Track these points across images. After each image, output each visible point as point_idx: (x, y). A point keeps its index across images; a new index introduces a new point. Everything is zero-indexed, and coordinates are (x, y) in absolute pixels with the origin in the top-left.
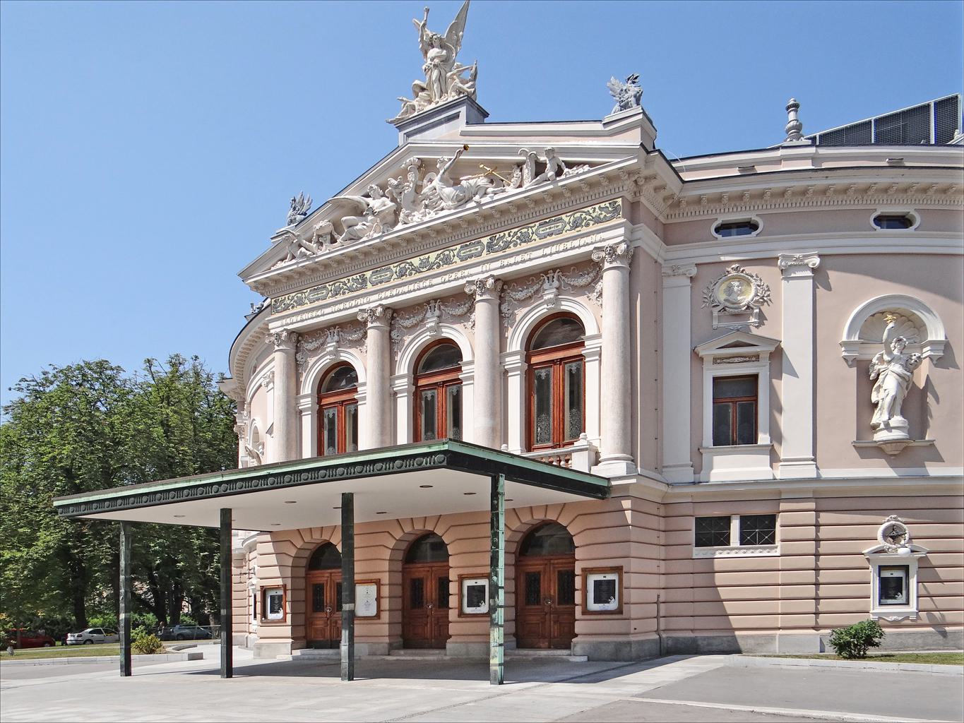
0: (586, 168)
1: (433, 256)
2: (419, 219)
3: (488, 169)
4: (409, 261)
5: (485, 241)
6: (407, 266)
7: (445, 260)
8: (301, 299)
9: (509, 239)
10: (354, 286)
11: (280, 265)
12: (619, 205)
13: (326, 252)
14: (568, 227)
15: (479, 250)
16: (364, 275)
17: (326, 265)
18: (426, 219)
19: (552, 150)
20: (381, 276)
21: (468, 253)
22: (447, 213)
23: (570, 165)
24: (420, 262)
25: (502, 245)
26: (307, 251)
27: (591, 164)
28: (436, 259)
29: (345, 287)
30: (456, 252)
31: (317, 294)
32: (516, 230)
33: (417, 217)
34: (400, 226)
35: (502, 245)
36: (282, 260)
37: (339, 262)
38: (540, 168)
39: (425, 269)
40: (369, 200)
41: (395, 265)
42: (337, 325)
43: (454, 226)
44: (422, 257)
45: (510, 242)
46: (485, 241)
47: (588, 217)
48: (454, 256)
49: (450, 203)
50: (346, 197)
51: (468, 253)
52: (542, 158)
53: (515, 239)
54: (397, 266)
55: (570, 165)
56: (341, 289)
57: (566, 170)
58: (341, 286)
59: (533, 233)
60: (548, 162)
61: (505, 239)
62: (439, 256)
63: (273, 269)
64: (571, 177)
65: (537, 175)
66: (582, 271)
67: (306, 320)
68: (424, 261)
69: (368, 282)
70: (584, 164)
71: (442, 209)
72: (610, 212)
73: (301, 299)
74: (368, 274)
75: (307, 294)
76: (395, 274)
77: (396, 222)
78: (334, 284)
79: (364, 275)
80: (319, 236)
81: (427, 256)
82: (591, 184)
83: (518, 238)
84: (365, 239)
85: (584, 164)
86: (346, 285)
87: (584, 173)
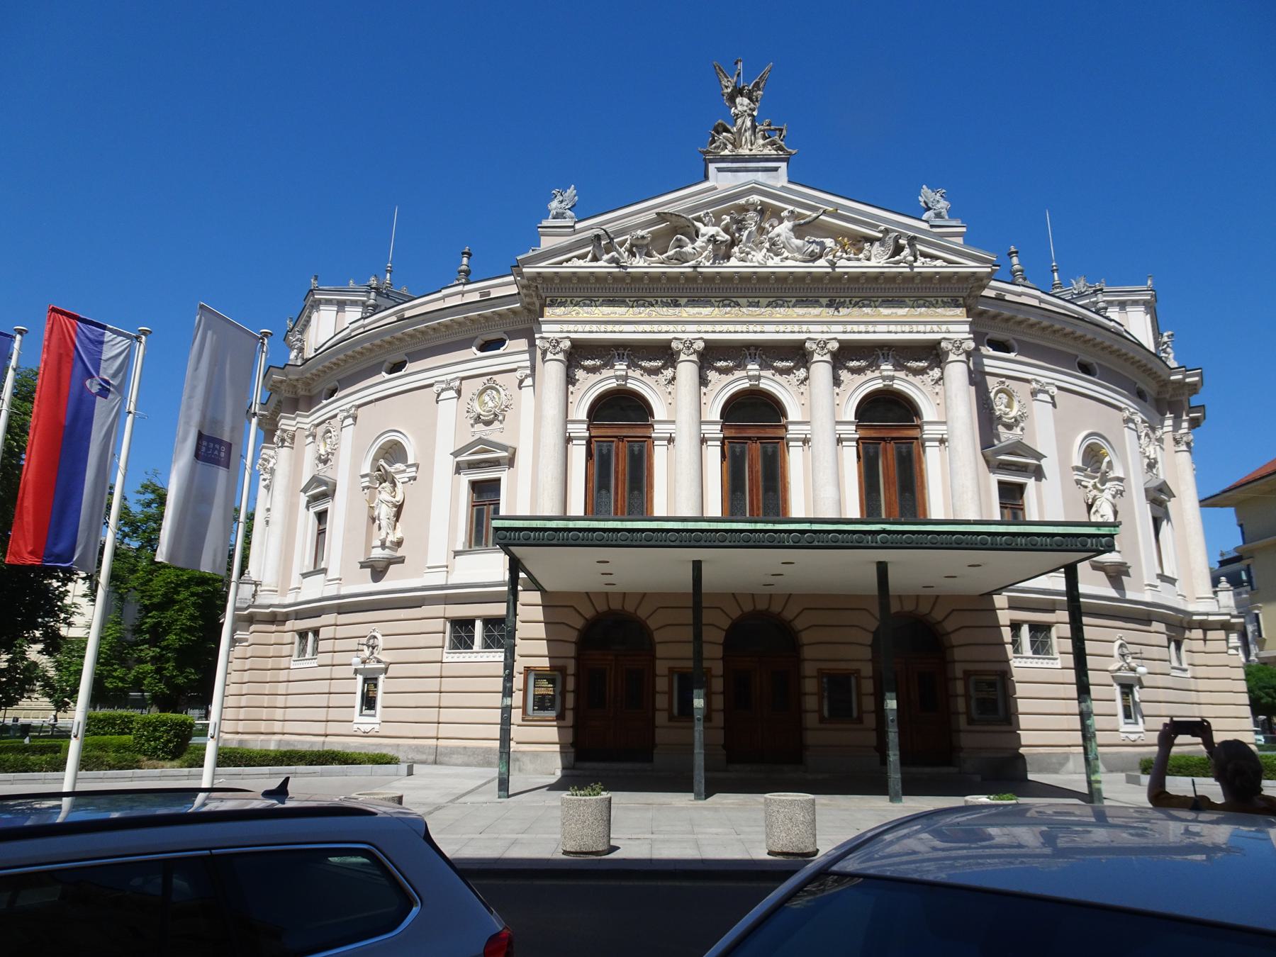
0: (939, 263)
2: (757, 260)
11: (576, 262)
13: (639, 264)
19: (914, 238)
23: (924, 255)
27: (945, 260)
33: (758, 256)
34: (733, 262)
36: (579, 257)
37: (654, 279)
49: (800, 257)
55: (924, 255)
64: (923, 266)
66: (932, 354)
70: (937, 258)
71: (787, 258)
77: (728, 257)
80: (632, 245)
85: (937, 258)
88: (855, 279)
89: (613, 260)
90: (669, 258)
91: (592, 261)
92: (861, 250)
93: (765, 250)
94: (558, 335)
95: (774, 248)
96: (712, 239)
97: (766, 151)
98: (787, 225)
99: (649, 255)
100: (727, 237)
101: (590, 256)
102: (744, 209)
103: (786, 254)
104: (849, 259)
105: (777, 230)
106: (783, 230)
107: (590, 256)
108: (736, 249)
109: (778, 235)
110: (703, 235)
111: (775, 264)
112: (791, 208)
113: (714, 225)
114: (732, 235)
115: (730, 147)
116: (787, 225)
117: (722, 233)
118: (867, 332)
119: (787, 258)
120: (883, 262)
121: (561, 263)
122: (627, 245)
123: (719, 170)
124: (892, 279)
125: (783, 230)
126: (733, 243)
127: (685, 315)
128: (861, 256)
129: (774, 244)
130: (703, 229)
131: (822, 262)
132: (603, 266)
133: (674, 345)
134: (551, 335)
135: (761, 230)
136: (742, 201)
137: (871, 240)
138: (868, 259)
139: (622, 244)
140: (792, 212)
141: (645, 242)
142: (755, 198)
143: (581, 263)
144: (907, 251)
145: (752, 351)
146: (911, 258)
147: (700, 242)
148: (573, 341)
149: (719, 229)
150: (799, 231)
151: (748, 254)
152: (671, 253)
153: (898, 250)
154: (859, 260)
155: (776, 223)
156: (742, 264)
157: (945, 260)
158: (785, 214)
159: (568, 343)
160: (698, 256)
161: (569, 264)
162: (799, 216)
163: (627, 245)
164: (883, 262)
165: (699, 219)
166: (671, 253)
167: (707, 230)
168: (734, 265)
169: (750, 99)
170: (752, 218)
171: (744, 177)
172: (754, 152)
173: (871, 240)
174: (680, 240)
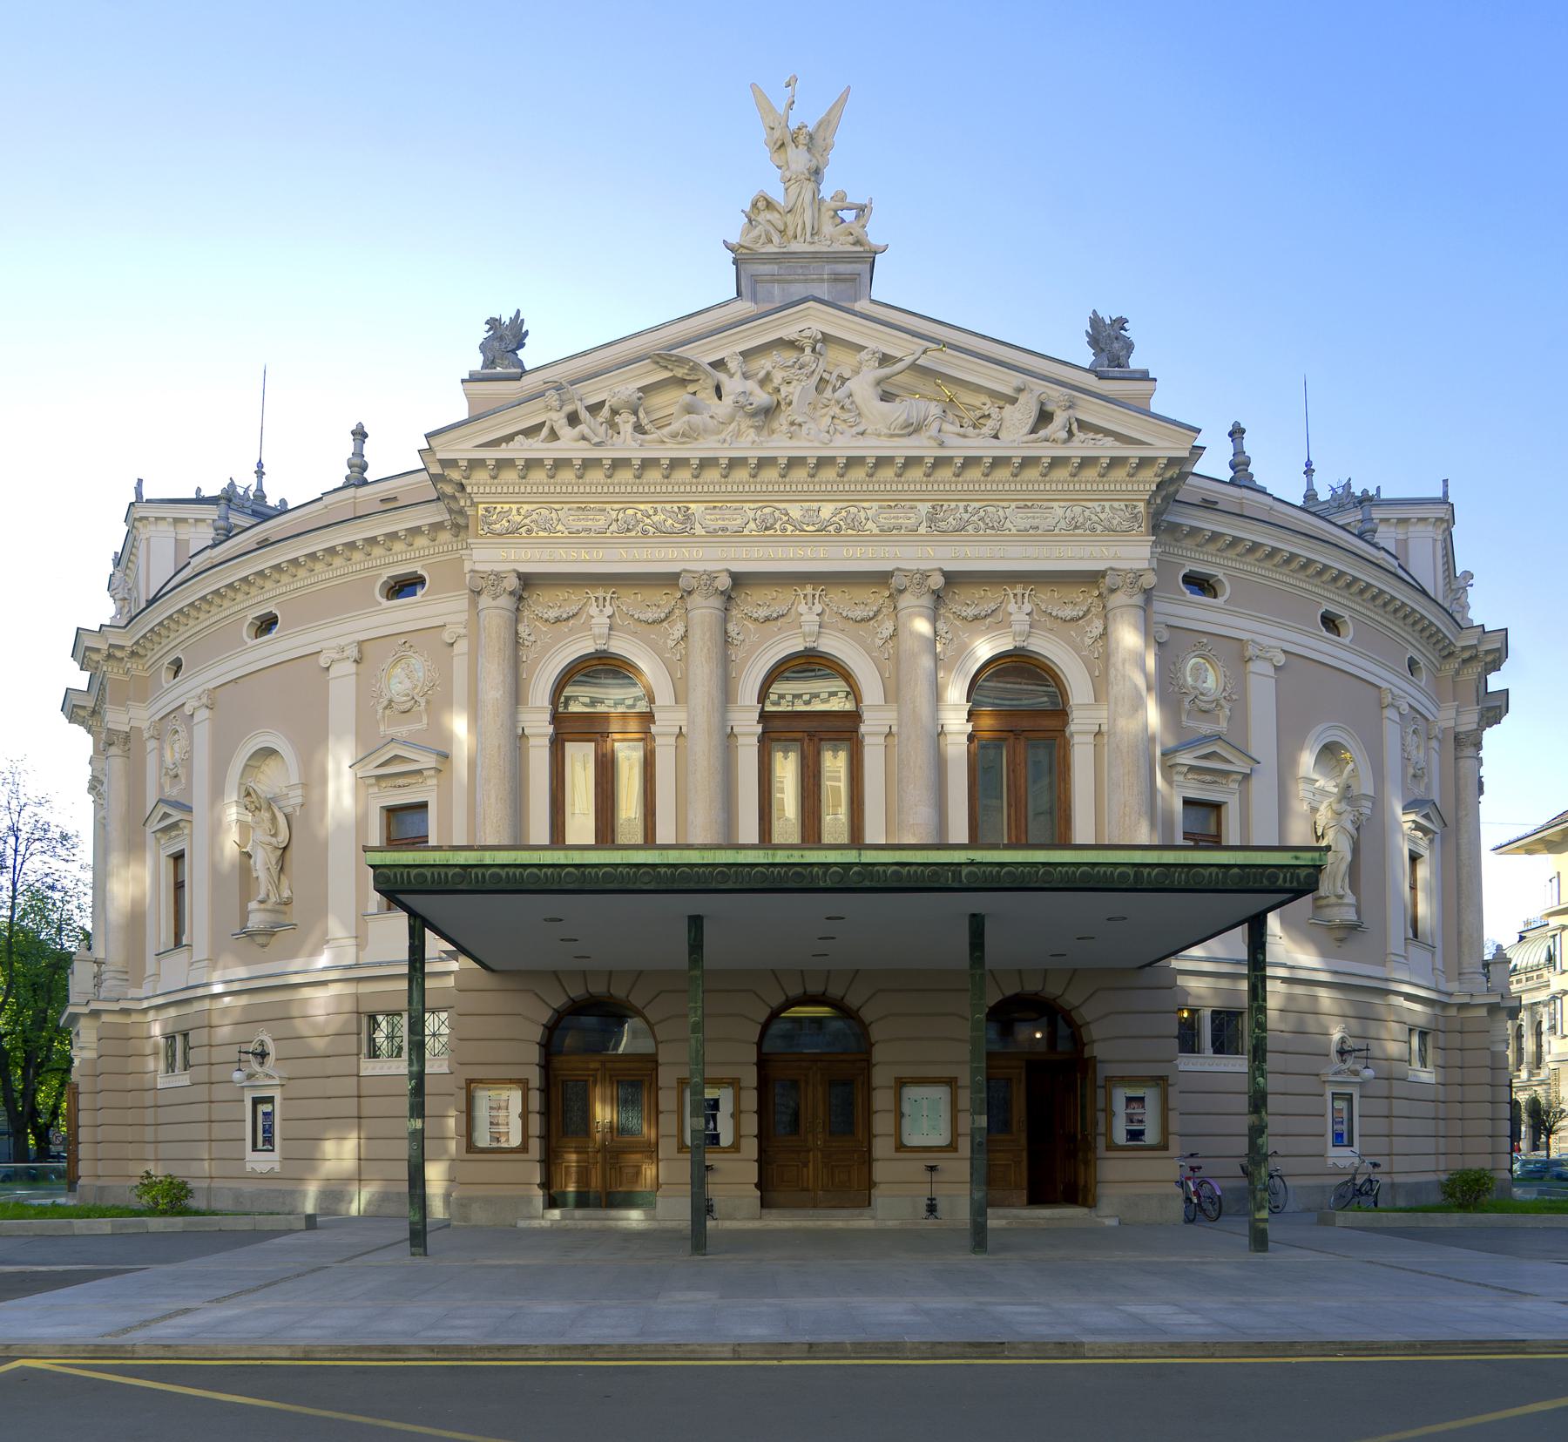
0: (1109, 441)
1: (827, 510)
6: (777, 514)
13: (627, 445)
14: (1063, 524)
22: (871, 447)
32: (977, 505)
40: (722, 377)
41: (752, 506)
44: (806, 505)
46: (924, 508)
47: (1095, 518)
53: (975, 518)
64: (1081, 447)
70: (1108, 433)
81: (815, 505)
85: (1108, 433)
87: (1107, 448)
93: (828, 420)
97: (837, 247)
106: (862, 387)
111: (844, 446)
115: (776, 238)
118: (992, 558)
138: (996, 437)
146: (1064, 435)
149: (751, 385)
153: (1044, 417)
156: (789, 443)
162: (885, 360)
167: (733, 386)
168: (780, 445)
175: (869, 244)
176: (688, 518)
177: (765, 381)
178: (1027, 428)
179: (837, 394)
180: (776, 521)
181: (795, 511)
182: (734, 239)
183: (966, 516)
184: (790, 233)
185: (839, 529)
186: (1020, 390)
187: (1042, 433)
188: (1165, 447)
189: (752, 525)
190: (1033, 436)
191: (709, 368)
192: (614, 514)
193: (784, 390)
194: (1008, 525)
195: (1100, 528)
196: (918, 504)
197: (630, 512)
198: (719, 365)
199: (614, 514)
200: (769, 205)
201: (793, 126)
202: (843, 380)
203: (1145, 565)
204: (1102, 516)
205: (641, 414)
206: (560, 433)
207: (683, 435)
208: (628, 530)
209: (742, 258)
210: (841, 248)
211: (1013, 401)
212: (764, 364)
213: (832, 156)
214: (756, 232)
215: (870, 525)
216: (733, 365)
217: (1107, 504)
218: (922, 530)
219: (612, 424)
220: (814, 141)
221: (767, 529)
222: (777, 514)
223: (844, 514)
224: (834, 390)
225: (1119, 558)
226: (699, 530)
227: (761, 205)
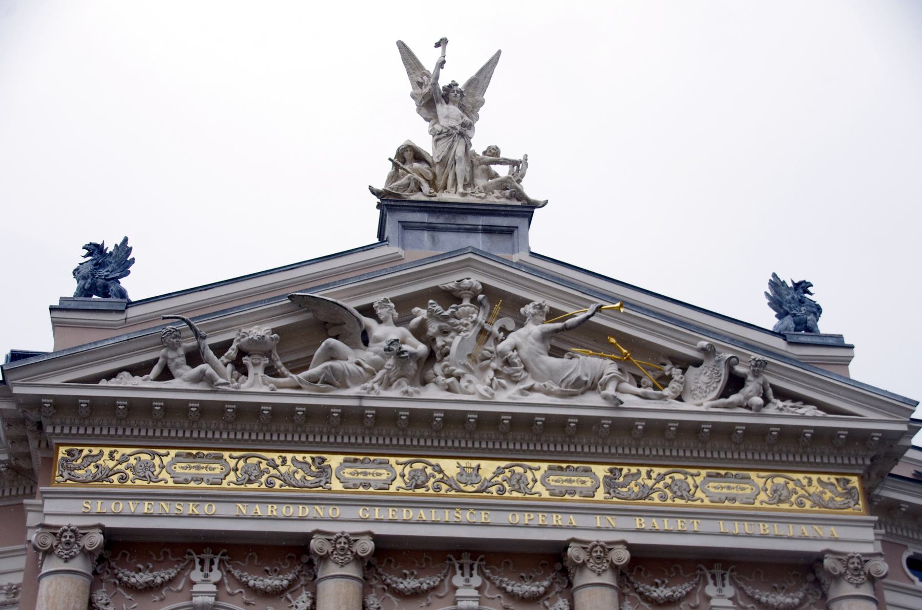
0: (809, 410)
1: (488, 468)
2: (477, 392)
3: (625, 351)
4: (433, 461)
5: (601, 471)
6: (429, 470)
7: (514, 482)
8: (149, 467)
9: (650, 483)
10: (298, 476)
11: (126, 380)
12: (854, 488)
13: (256, 387)
15: (589, 484)
16: (324, 460)
17: (248, 413)
18: (502, 397)
20: (365, 474)
21: (565, 484)
22: (540, 403)
23: (782, 394)
24: (459, 470)
25: (636, 489)
26: (217, 376)
27: (820, 406)
28: (496, 474)
29: (273, 472)
30: (538, 475)
31: (198, 468)
32: (663, 471)
34: (432, 392)
35: (636, 489)
36: (139, 370)
37: (282, 414)
38: (735, 383)
39: (470, 488)
40: (368, 321)
42: (224, 546)
43: (556, 427)
44: (463, 463)
45: (652, 489)
47: (801, 492)
48: (535, 481)
49: (556, 388)
50: (339, 302)
51: (565, 484)
52: (740, 369)
53: (661, 485)
54: (406, 464)
55: (782, 394)
56: (262, 473)
57: (780, 404)
58: (263, 466)
59: (696, 487)
60: (750, 378)
61: (640, 481)
62: (499, 472)
63: (104, 383)
64: (779, 415)
65: (724, 394)
67: (160, 516)
68: (470, 471)
69: (334, 476)
70: (807, 401)
71: (531, 389)
72: (840, 495)
73: (149, 467)
74: (335, 461)
75: (166, 460)
76: (399, 478)
78: (246, 458)
79: (324, 460)
80: (241, 353)
81: (474, 463)
82: (823, 438)
83: (667, 486)
84: (355, 390)
85: (807, 401)
86: (275, 467)
87: (807, 417)
88: (657, 430)
89: (202, 378)
90: (313, 380)
91: (158, 379)
92: (665, 380)
93: (491, 374)
94: (76, 522)
95: (509, 369)
96: (394, 350)
98: (533, 329)
99: (271, 371)
100: (422, 348)
101: (156, 370)
102: (450, 297)
103: (529, 383)
104: (645, 397)
105: (511, 339)
107: (156, 370)
108: (438, 368)
109: (515, 348)
110: (378, 340)
111: (509, 398)
112: (538, 300)
113: (397, 323)
114: (430, 341)
115: (426, 187)
116: (533, 329)
117: (412, 339)
119: (531, 389)
120: (706, 405)
121: (95, 379)
122: (232, 352)
123: (406, 226)
124: (723, 432)
125: (527, 336)
126: (432, 357)
127: (336, 485)
128: (666, 392)
129: (508, 362)
130: (378, 331)
131: (593, 399)
132: (183, 386)
133: (314, 544)
134: (63, 522)
135: (484, 334)
136: (448, 282)
137: (684, 363)
138: (680, 399)
139: (220, 349)
140: (541, 307)
141: (266, 349)
142: (474, 280)
143: (138, 381)
144: (751, 386)
145: (466, 561)
146: (758, 400)
147: (369, 355)
148: (108, 533)
150: (558, 343)
151: (459, 378)
152: (313, 371)
153: (735, 383)
154: (663, 398)
155: (510, 325)
157: (820, 406)
158: (528, 309)
159: (97, 538)
160: (361, 377)
161: (113, 382)
162: (553, 314)
163: (232, 352)
164: (706, 405)
165: (368, 310)
166: (313, 371)
167: (385, 332)
168: (433, 396)
169: (462, 107)
170: (467, 315)
171: (450, 241)
172: (470, 199)
173: (684, 363)
174: (330, 348)
175: (527, 199)
176: (324, 471)
177: (420, 332)
178: (715, 393)
179: (500, 346)
180: (428, 478)
181: (450, 467)
182: (380, 186)
183: (650, 483)
184: (440, 183)
185: (502, 491)
186: (703, 350)
187: (734, 398)
188: (873, 421)
189: (399, 482)
190: (723, 400)
191: (356, 313)
192: (232, 463)
193: (440, 342)
194: (699, 494)
195: (808, 504)
196: (594, 467)
197: (254, 461)
198: (368, 310)
199: (232, 463)
200: (418, 156)
201: (443, 82)
202: (506, 332)
203: (869, 549)
204: (811, 490)
205: (276, 355)
206: (176, 372)
207: (324, 382)
208: (250, 481)
209: (389, 202)
210: (498, 201)
211: (697, 364)
212: (421, 314)
213: (482, 112)
214: (403, 181)
215: (539, 487)
216: (382, 312)
217: (814, 477)
218: (600, 495)
219: (241, 369)
220: (468, 97)
221: (417, 486)
222: (429, 470)
223: (508, 473)
224: (497, 341)
225: (837, 540)
226: (336, 485)
227: (408, 155)
